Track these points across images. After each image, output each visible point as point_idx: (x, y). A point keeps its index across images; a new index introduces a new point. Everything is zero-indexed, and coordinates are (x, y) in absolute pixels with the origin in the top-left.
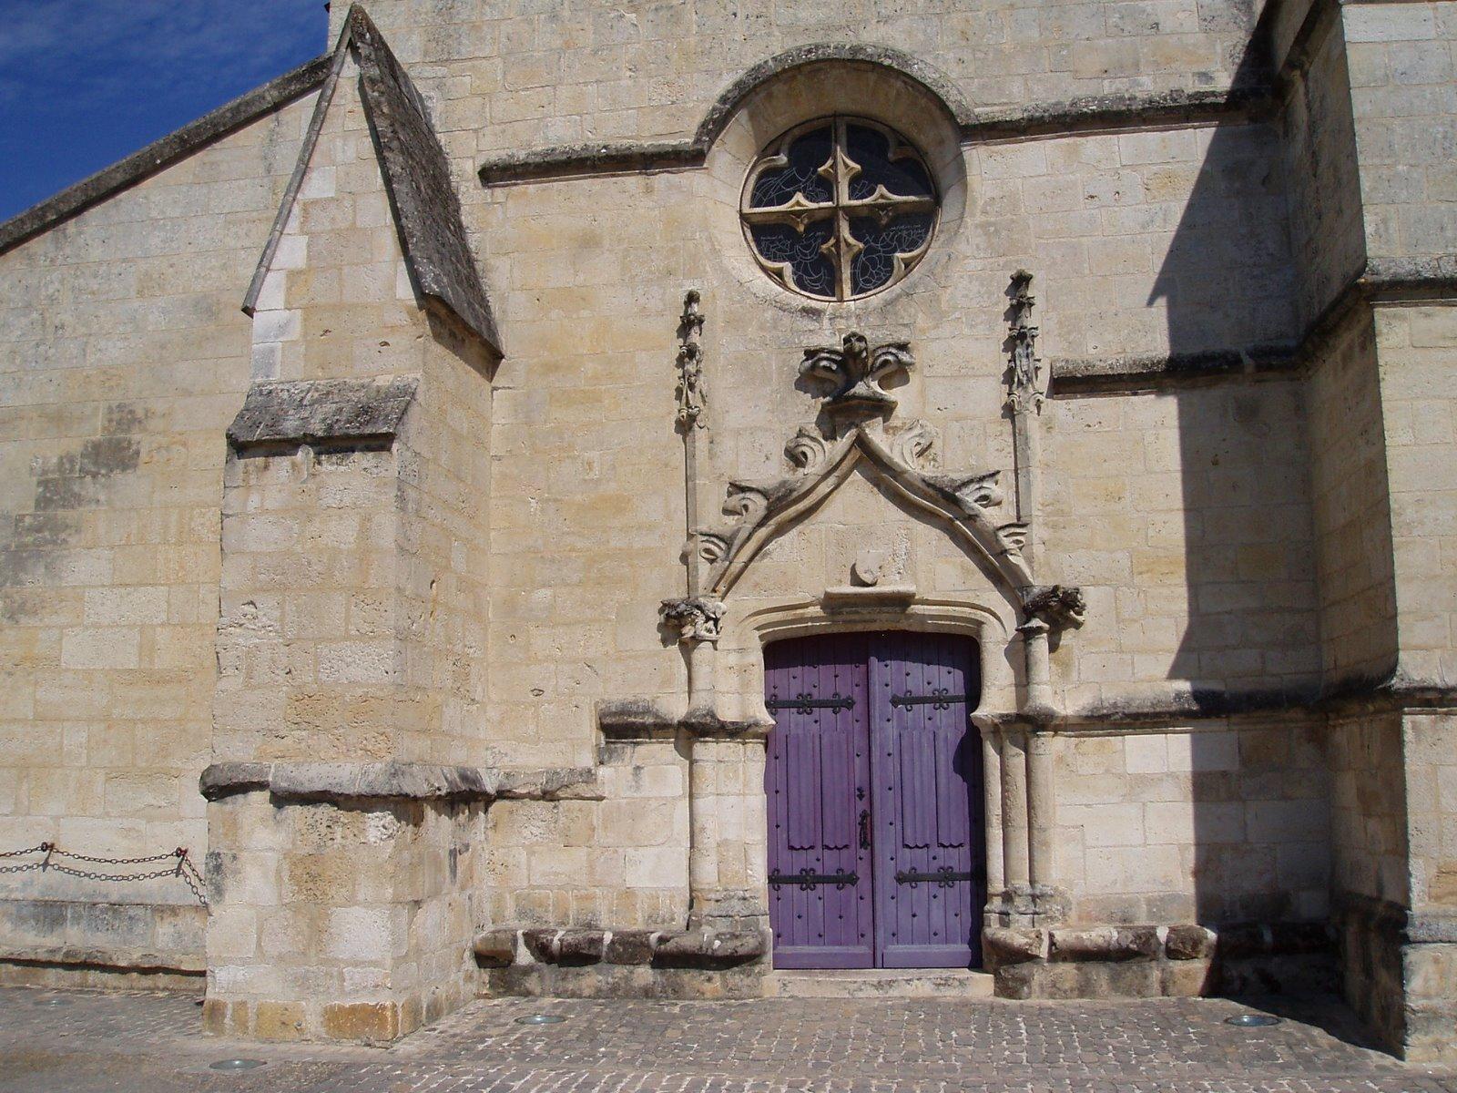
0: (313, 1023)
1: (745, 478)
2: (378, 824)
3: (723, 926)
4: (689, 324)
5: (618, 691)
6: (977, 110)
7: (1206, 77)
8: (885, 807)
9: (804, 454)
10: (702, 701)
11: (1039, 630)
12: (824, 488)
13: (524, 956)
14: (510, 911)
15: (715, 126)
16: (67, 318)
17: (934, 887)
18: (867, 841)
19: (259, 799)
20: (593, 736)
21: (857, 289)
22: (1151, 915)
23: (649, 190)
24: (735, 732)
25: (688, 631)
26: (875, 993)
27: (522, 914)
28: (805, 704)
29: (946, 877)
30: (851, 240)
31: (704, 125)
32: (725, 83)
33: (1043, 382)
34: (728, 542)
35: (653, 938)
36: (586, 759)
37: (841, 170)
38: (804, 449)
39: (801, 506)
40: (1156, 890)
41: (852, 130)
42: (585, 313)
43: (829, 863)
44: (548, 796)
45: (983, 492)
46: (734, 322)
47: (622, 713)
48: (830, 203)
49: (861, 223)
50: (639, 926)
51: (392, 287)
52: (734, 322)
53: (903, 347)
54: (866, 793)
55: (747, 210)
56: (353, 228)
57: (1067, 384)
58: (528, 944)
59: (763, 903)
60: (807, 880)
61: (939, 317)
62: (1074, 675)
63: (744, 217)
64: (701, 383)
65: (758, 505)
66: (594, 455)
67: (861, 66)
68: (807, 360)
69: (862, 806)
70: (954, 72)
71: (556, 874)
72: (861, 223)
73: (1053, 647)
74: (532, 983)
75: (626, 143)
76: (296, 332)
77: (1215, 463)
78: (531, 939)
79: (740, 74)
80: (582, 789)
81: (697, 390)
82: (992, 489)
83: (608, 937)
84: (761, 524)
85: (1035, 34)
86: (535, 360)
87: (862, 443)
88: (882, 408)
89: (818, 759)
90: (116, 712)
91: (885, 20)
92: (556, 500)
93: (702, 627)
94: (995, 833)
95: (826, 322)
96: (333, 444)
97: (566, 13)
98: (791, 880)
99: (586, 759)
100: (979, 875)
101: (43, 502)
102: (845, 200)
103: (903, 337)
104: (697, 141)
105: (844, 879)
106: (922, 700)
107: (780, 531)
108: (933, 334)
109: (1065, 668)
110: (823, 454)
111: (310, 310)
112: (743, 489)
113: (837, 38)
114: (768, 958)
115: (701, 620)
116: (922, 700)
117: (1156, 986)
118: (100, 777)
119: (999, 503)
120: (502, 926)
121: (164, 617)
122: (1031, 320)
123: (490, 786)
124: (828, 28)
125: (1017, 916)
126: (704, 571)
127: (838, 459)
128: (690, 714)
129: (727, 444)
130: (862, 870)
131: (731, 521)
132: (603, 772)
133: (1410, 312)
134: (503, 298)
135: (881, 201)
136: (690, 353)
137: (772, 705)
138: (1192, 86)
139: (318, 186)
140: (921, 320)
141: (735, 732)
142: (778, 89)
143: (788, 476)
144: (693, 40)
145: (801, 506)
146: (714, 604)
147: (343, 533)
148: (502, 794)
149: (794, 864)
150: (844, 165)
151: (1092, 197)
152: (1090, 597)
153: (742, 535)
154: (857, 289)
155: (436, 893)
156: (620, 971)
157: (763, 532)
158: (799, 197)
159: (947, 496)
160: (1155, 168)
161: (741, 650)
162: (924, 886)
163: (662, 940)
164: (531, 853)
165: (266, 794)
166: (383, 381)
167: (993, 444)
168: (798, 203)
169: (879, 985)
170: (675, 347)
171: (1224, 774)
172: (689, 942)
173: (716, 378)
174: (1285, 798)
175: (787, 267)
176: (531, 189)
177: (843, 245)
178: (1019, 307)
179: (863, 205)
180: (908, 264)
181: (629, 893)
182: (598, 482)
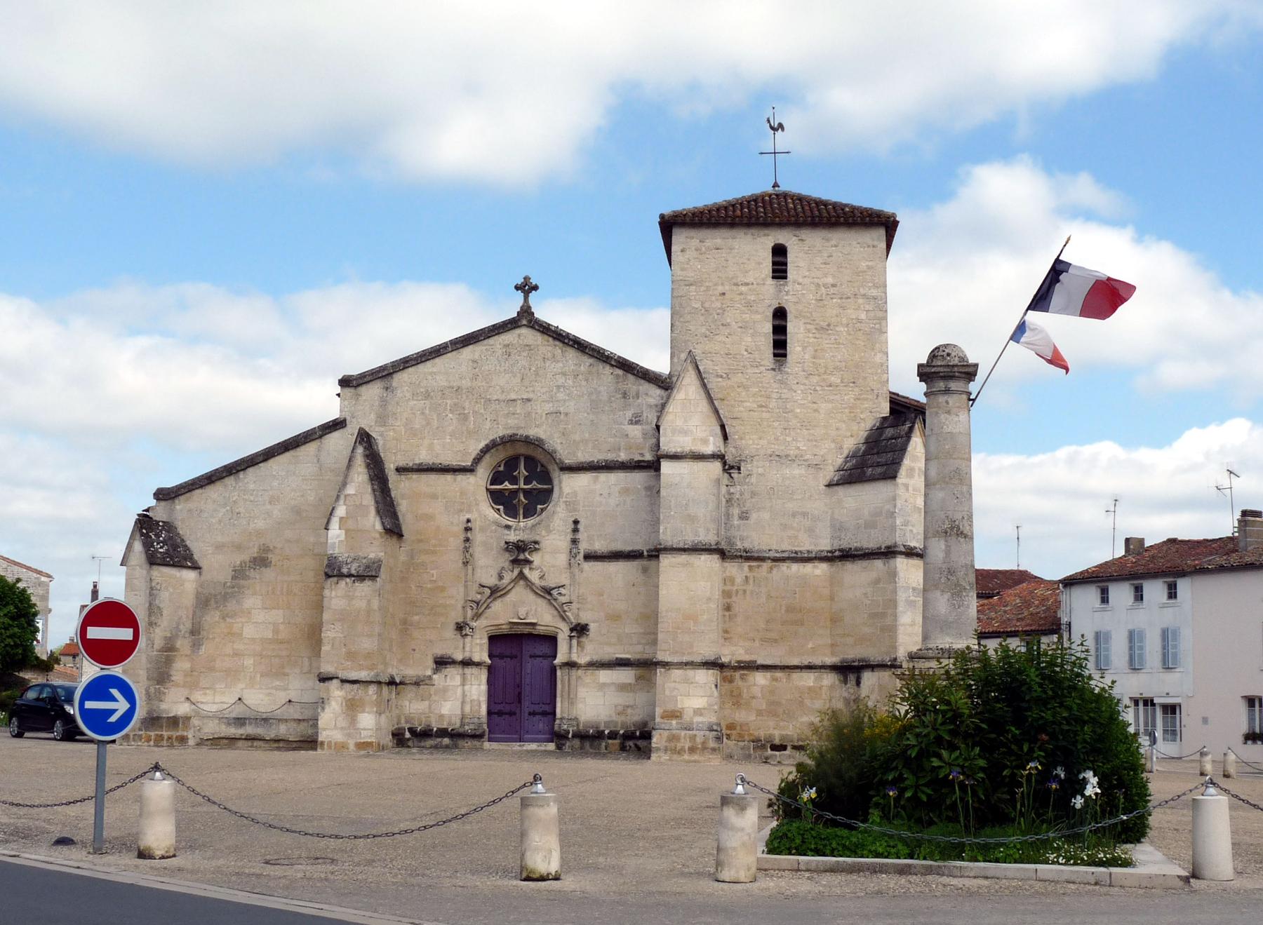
0: (352, 747)
1: (485, 582)
2: (372, 689)
3: (472, 727)
4: (467, 529)
5: (440, 651)
6: (566, 461)
7: (642, 455)
8: (526, 690)
10: (467, 655)
11: (574, 636)
12: (509, 587)
13: (408, 735)
14: (403, 721)
15: (477, 460)
16: (241, 510)
18: (520, 702)
19: (335, 681)
20: (433, 665)
21: (524, 518)
22: (605, 727)
23: (455, 480)
24: (478, 664)
25: (464, 633)
26: (519, 748)
27: (407, 722)
28: (501, 657)
29: (544, 714)
30: (524, 500)
31: (474, 459)
32: (482, 445)
33: (581, 555)
34: (478, 604)
35: (450, 729)
36: (429, 673)
37: (521, 474)
39: (502, 593)
40: (606, 719)
43: (508, 708)
44: (417, 684)
46: (483, 529)
47: (441, 658)
48: (515, 487)
50: (445, 726)
51: (374, 525)
52: (483, 529)
53: (536, 542)
54: (519, 686)
55: (489, 487)
56: (361, 504)
57: (589, 557)
58: (409, 731)
59: (484, 720)
60: (500, 713)
61: (549, 532)
63: (487, 489)
64: (471, 550)
65: (488, 592)
66: (434, 572)
67: (527, 441)
70: (559, 448)
72: (527, 493)
73: (579, 643)
74: (410, 743)
75: (448, 463)
76: (343, 537)
78: (410, 730)
79: (487, 442)
80: (427, 682)
82: (562, 590)
83: (435, 729)
84: (488, 598)
85: (587, 435)
87: (521, 573)
88: (528, 562)
90: (264, 653)
91: (537, 426)
93: (468, 631)
94: (559, 700)
95: (512, 532)
96: (360, 577)
97: (427, 412)
98: (495, 713)
99: (429, 673)
100: (554, 713)
101: (234, 578)
103: (537, 538)
104: (472, 465)
105: (511, 714)
106: (540, 656)
107: (495, 599)
108: (547, 538)
109: (583, 648)
110: (508, 577)
111: (347, 531)
112: (484, 587)
113: (520, 432)
114: (487, 736)
116: (540, 656)
117: (604, 748)
118: (259, 676)
120: (400, 726)
121: (282, 620)
123: (398, 681)
124: (518, 428)
126: (470, 613)
128: (463, 659)
129: (479, 572)
130: (518, 711)
131: (479, 596)
132: (434, 676)
133: (669, 556)
134: (403, 515)
136: (467, 540)
137: (490, 656)
138: (638, 458)
139: (350, 490)
140: (544, 533)
141: (478, 664)
143: (497, 582)
144: (472, 426)
145: (502, 593)
146: (474, 624)
147: (362, 604)
148: (402, 683)
150: (522, 471)
152: (592, 627)
153: (482, 602)
154: (525, 517)
155: (384, 712)
156: (439, 740)
157: (489, 600)
158: (506, 483)
159: (548, 591)
161: (481, 638)
162: (537, 716)
163: (452, 730)
164: (410, 702)
166: (372, 556)
167: (564, 576)
169: (520, 746)
170: (462, 537)
171: (630, 684)
172: (461, 730)
173: (477, 550)
174: (648, 692)
176: (415, 476)
178: (575, 530)
180: (542, 510)
181: (442, 716)
182: (435, 581)
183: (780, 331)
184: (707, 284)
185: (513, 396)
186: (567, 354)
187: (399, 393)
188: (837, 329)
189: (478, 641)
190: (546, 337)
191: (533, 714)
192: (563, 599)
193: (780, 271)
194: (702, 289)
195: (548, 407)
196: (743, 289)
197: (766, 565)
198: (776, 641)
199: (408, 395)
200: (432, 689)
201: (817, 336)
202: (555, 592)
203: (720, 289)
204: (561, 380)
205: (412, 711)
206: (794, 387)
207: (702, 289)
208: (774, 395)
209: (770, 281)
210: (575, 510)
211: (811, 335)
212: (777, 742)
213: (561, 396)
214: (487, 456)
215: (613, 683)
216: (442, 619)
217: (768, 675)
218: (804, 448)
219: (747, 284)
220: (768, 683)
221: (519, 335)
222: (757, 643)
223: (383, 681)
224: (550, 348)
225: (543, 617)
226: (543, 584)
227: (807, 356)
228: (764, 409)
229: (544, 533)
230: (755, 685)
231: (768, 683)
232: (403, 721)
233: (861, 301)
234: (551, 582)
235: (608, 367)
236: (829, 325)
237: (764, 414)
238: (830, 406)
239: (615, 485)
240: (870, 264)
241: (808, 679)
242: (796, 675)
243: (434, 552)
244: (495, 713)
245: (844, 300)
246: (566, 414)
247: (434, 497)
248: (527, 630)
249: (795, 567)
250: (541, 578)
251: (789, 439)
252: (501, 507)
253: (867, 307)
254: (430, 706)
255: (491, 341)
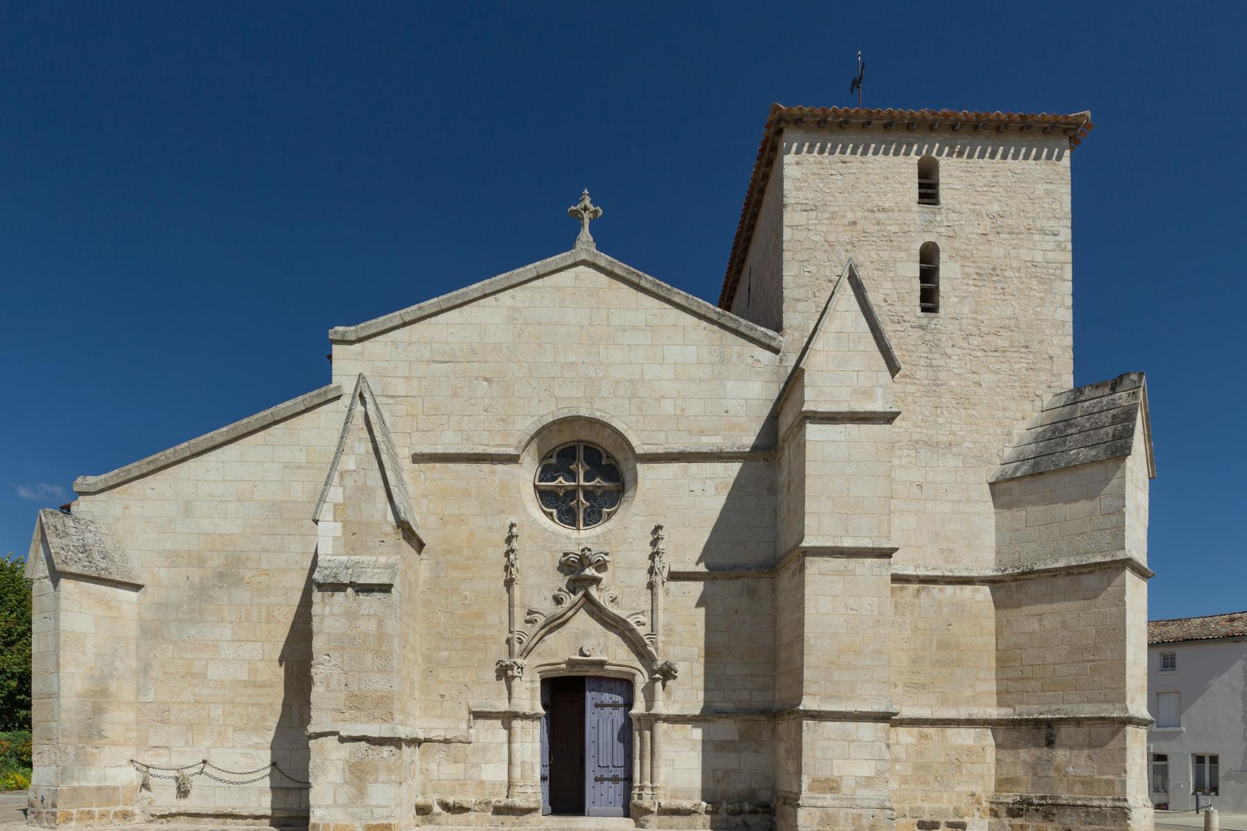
9: (562, 599)
11: (658, 679)
12: (570, 614)
13: (437, 809)
17: (610, 784)
21: (585, 524)
30: (584, 501)
38: (562, 596)
41: (586, 448)
42: (464, 527)
45: (638, 620)
49: (589, 494)
55: (537, 483)
57: (675, 576)
62: (673, 698)
63: (535, 487)
67: (592, 422)
68: (564, 557)
71: (451, 774)
73: (664, 686)
74: (439, 819)
77: (736, 612)
81: (515, 567)
84: (542, 628)
86: (441, 548)
87: (587, 596)
88: (596, 581)
90: (238, 700)
92: (450, 612)
94: (637, 762)
100: (629, 779)
102: (582, 482)
106: (608, 705)
109: (669, 695)
115: (516, 668)
116: (608, 705)
118: (231, 730)
119: (644, 625)
121: (261, 657)
122: (661, 545)
125: (646, 795)
127: (576, 601)
135: (598, 484)
151: (692, 491)
154: (585, 524)
157: (543, 631)
158: (561, 479)
160: (720, 480)
161: (532, 681)
165: (337, 737)
167: (643, 599)
168: (560, 482)
171: (732, 741)
174: (756, 752)
175: (555, 511)
177: (580, 503)
179: (590, 486)
182: (469, 605)
183: (929, 274)
184: (832, 209)
188: (1006, 274)
193: (928, 192)
194: (826, 215)
196: (880, 216)
197: (912, 587)
198: (924, 686)
201: (979, 283)
203: (850, 216)
205: (442, 777)
206: (949, 351)
207: (826, 215)
208: (923, 362)
209: (916, 207)
211: (971, 282)
212: (926, 818)
215: (710, 740)
216: (480, 655)
217: (915, 730)
218: (962, 433)
219: (884, 210)
220: (914, 741)
221: (577, 277)
222: (900, 689)
225: (615, 653)
227: (966, 310)
228: (908, 380)
230: (898, 743)
231: (914, 741)
233: (1036, 237)
236: (994, 269)
237: (909, 386)
238: (995, 377)
239: (711, 479)
240: (1050, 187)
241: (965, 737)
242: (951, 732)
245: (1014, 236)
248: (593, 672)
249: (949, 589)
251: (940, 420)
252: (555, 511)
253: (1045, 246)
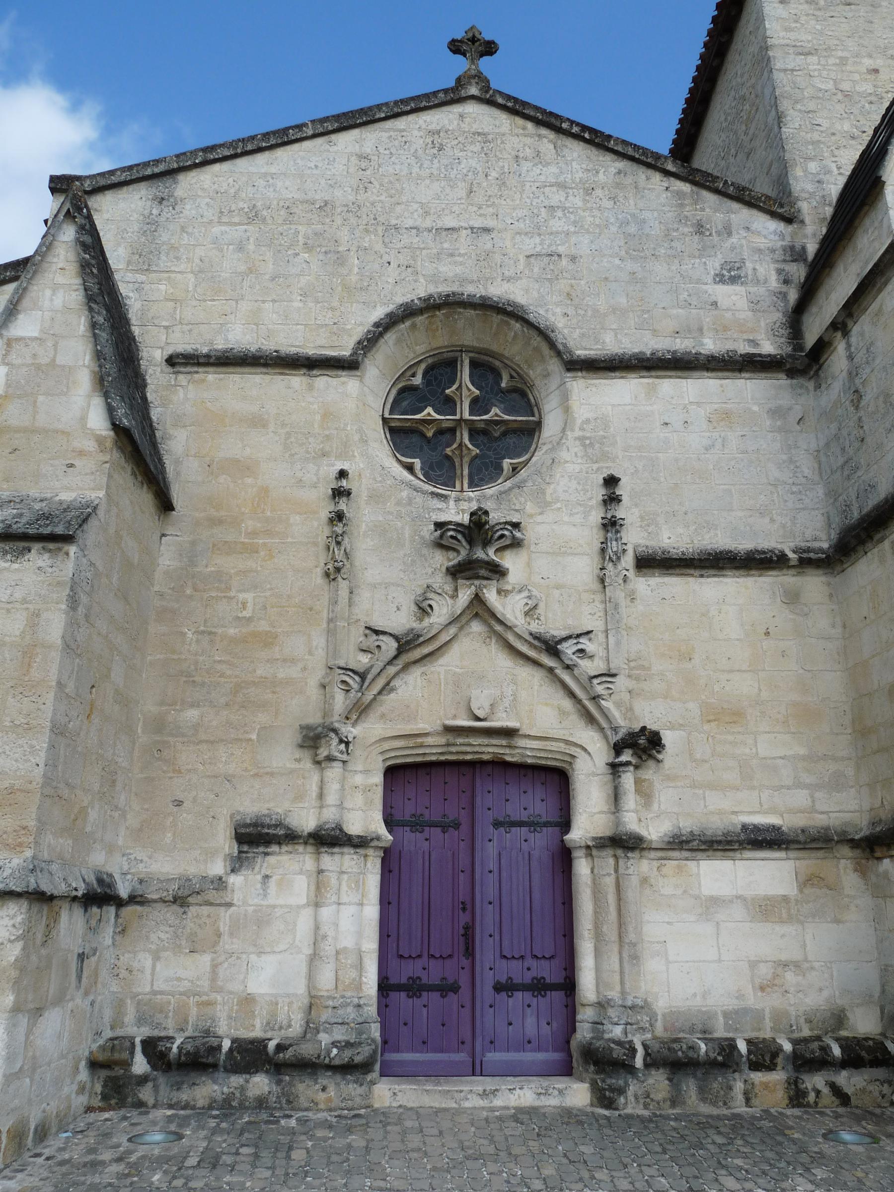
1: (379, 624)
3: (339, 1034)
4: (339, 493)
6: (578, 352)
7: (754, 343)
8: (487, 919)
9: (430, 606)
10: (330, 815)
12: (444, 638)
13: (140, 1065)
14: (130, 1017)
17: (528, 995)
18: (470, 951)
20: (229, 846)
21: (472, 484)
22: (728, 1028)
23: (311, 388)
24: (360, 843)
25: (323, 752)
26: (481, 1103)
27: (141, 1021)
28: (417, 824)
29: (539, 987)
30: (470, 446)
31: (359, 343)
32: (379, 313)
33: (628, 561)
34: (363, 676)
35: (272, 1045)
36: (218, 868)
37: (465, 392)
38: (431, 602)
39: (426, 650)
40: (731, 1004)
41: (474, 364)
42: (249, 481)
43: (434, 973)
44: (180, 901)
45: (580, 647)
46: (375, 497)
47: (255, 825)
49: (477, 432)
50: (257, 1033)
51: (83, 419)
52: (375, 497)
53: (516, 525)
54: (467, 906)
55: (387, 415)
56: (53, 363)
58: (145, 1052)
59: (372, 1010)
60: (414, 988)
61: (544, 505)
62: (655, 806)
63: (385, 420)
64: (346, 542)
65: (390, 646)
66: (249, 596)
68: (436, 530)
69: (464, 918)
71: (179, 979)
74: (146, 1094)
75: (293, 350)
77: (767, 634)
78: (151, 1046)
79: (391, 308)
80: (211, 895)
81: (343, 548)
82: (585, 643)
83: (226, 1044)
84: (390, 663)
85: (623, 301)
86: (202, 515)
87: (478, 599)
89: (427, 873)
92: (210, 633)
93: (333, 747)
95: (452, 503)
97: (251, 247)
98: (399, 988)
99: (218, 868)
100: (569, 986)
102: (467, 416)
104: (354, 353)
105: (447, 988)
106: (520, 824)
107: (406, 667)
108: (539, 519)
112: (377, 632)
114: (377, 1067)
115: (335, 741)
116: (520, 824)
117: (740, 1098)
119: (591, 657)
120: (119, 1032)
122: (620, 512)
123: (123, 892)
124: (464, 281)
125: (610, 1027)
126: (340, 701)
127: (459, 612)
128: (320, 828)
129: (364, 597)
130: (464, 981)
131: (365, 659)
132: (235, 880)
134: (177, 462)
135: (496, 418)
136: (339, 516)
137: (390, 822)
138: (744, 348)
140: (530, 508)
141: (360, 843)
142: (420, 319)
143: (415, 625)
144: (354, 278)
145: (426, 650)
146: (350, 731)
148: (134, 899)
149: (404, 972)
151: (667, 424)
152: (668, 737)
153: (375, 671)
154: (472, 484)
155: (60, 1000)
156: (236, 1080)
157: (392, 670)
158: (429, 410)
159: (552, 647)
160: (716, 406)
162: (519, 995)
163: (280, 1048)
164: (156, 958)
166: (66, 496)
168: (429, 414)
169: (484, 1094)
170: (325, 511)
171: (785, 899)
172: (307, 1050)
174: (837, 921)
175: (417, 463)
176: (211, 376)
177: (464, 448)
178: (612, 500)
179: (481, 420)
180: (515, 469)
181: (248, 1000)
182: (249, 620)
184: (840, 54)
185: (450, 222)
186: (566, 151)
187: (189, 210)
189: (359, 779)
190: (520, 121)
191: (505, 988)
192: (588, 667)
194: (831, 61)
195: (531, 244)
199: (209, 214)
200: (225, 917)
202: (568, 649)
203: (868, 63)
204: (556, 197)
205: (160, 985)
210: (605, 456)
213: (557, 224)
214: (390, 337)
215: (738, 897)
216: (263, 718)
223: (61, 889)
224: (528, 141)
226: (535, 627)
229: (530, 508)
232: (130, 1017)
234: (554, 628)
235: (657, 177)
239: (698, 404)
243: (252, 550)
244: (399, 988)
246: (573, 259)
247: (258, 422)
248: (489, 749)
250: (530, 612)
252: (417, 463)
254: (215, 967)
255: (401, 123)
